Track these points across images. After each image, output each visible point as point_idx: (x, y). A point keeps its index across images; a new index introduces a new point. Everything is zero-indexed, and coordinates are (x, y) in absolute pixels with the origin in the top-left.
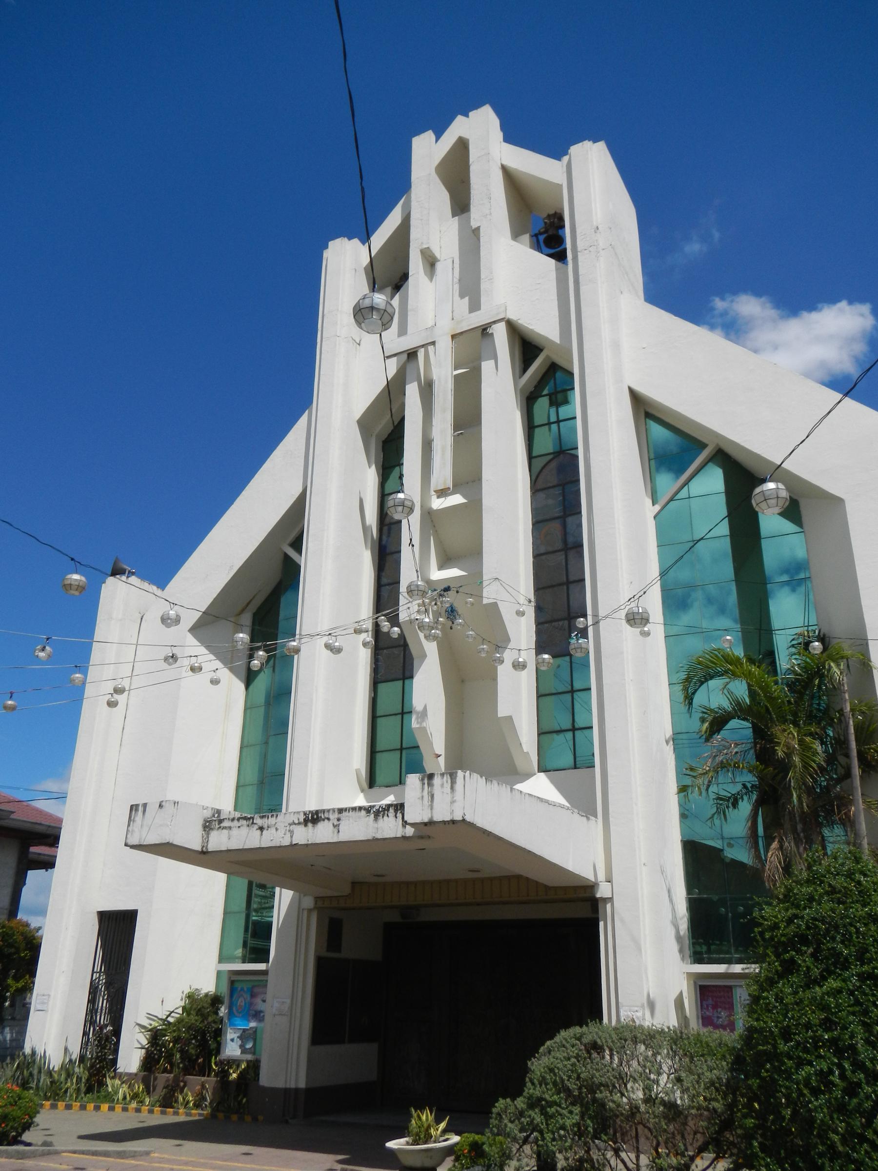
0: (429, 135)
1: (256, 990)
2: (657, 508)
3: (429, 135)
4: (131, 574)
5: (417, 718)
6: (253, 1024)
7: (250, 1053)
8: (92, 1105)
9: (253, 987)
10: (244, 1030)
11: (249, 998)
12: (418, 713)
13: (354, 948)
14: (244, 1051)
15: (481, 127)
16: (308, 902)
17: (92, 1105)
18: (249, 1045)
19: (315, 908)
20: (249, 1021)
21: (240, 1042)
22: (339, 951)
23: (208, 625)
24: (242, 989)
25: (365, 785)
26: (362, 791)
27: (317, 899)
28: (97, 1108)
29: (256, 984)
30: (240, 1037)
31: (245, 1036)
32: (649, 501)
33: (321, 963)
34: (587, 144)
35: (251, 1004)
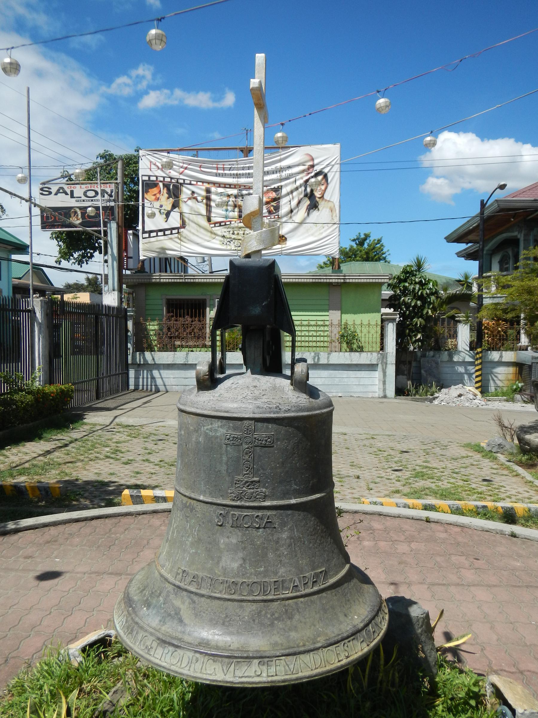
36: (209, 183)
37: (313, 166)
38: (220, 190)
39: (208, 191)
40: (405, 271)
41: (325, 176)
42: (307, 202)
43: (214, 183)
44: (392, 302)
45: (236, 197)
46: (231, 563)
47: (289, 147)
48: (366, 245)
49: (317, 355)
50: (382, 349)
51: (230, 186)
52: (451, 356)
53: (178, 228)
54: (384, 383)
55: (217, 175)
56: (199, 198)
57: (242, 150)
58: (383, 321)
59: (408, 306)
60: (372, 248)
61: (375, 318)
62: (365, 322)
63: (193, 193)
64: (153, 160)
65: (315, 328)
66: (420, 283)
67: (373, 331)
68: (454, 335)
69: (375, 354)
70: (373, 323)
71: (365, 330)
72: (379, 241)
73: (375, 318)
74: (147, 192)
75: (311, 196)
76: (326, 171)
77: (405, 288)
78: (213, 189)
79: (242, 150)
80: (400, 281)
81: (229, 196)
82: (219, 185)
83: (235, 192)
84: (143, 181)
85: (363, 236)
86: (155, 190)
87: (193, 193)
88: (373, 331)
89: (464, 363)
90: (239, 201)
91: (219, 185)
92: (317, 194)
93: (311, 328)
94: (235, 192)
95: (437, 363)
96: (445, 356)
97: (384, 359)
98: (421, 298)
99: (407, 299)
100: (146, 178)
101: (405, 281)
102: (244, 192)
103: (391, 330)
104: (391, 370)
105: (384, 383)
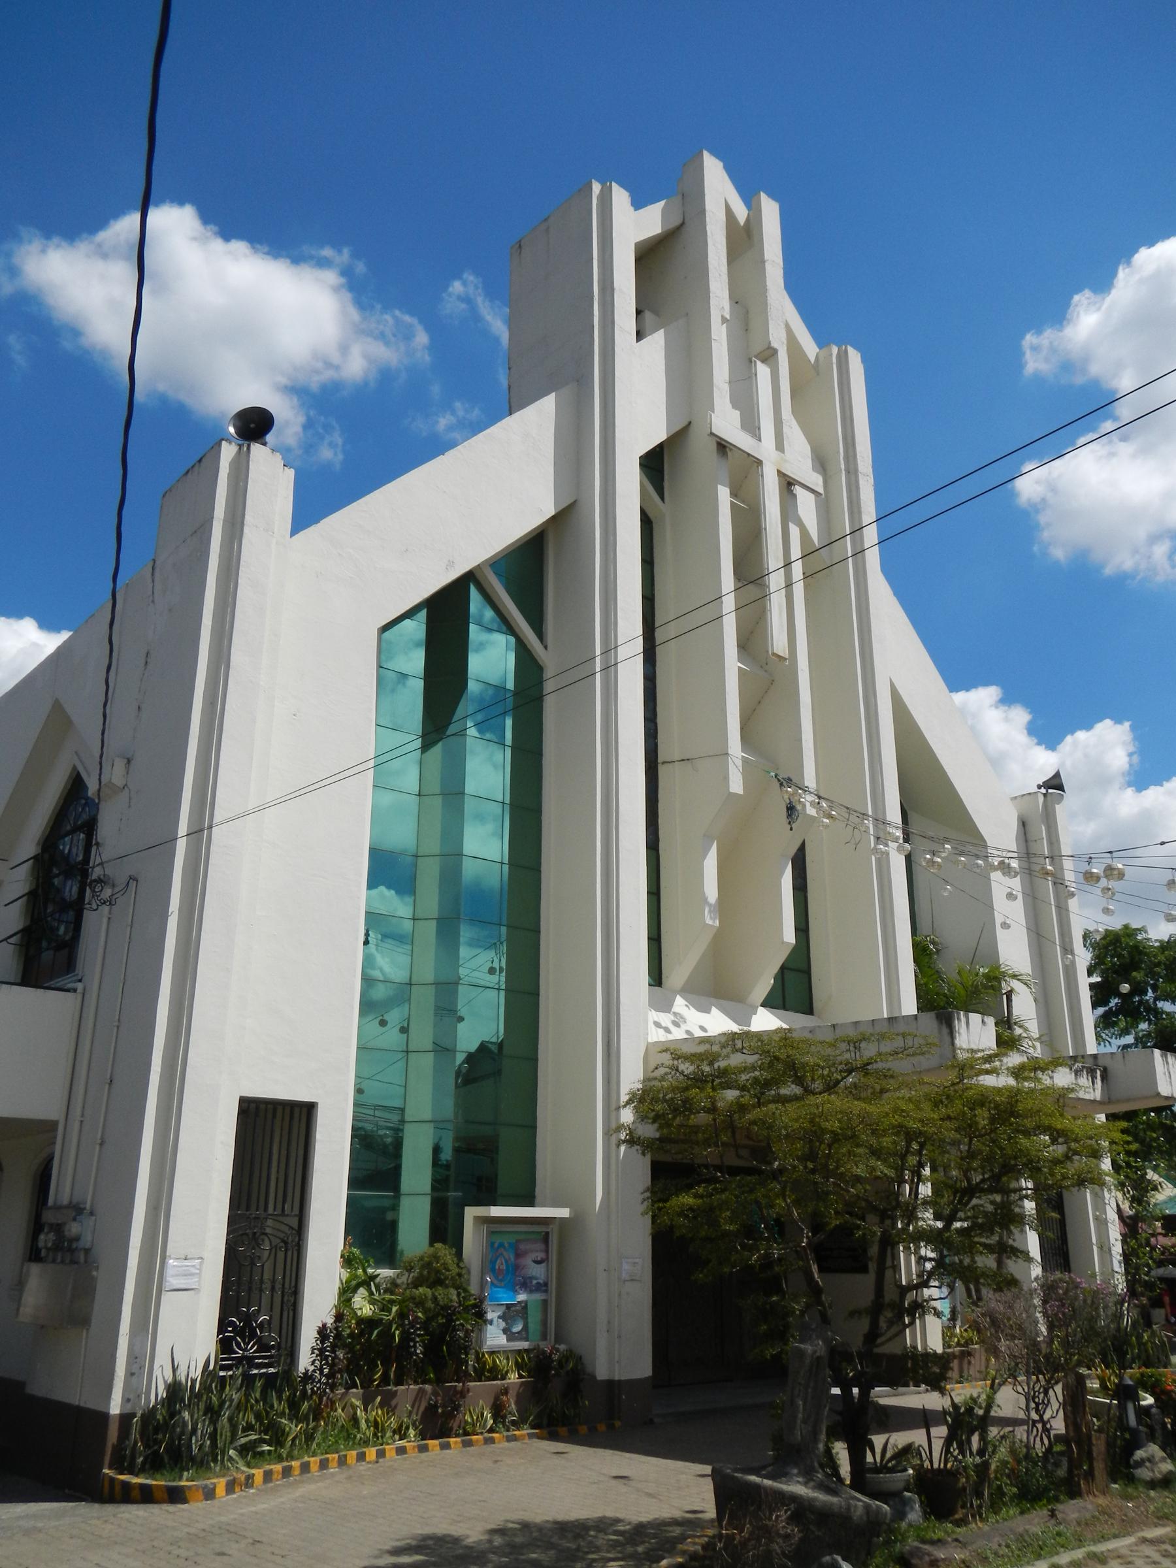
1: (522, 1247)
5: (710, 912)
6: (522, 1297)
7: (521, 1339)
8: (354, 1453)
9: (518, 1241)
10: (508, 1306)
11: (512, 1257)
12: (710, 905)
14: (511, 1337)
17: (354, 1453)
18: (517, 1328)
20: (516, 1292)
21: (503, 1324)
24: (501, 1245)
28: (342, 1462)
29: (522, 1237)
30: (503, 1317)
31: (509, 1313)
35: (517, 1268)
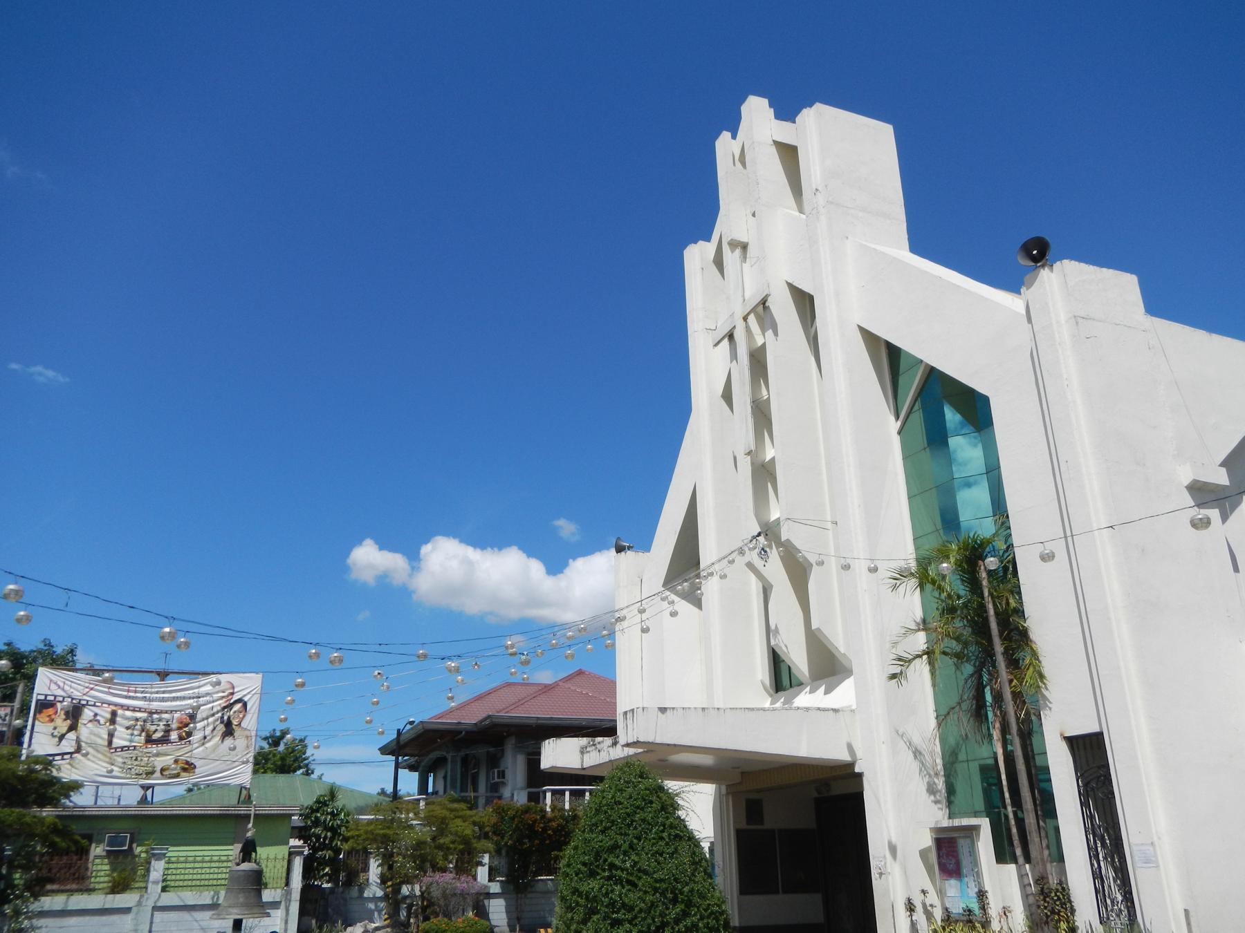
0: (726, 135)
2: (899, 423)
3: (726, 135)
4: (629, 548)
13: (773, 820)
15: (757, 112)
16: (724, 788)
19: (728, 794)
22: (762, 823)
23: (671, 580)
25: (772, 692)
26: (771, 696)
27: (728, 786)
32: (892, 418)
33: (740, 834)
34: (805, 111)
36: (116, 705)
37: (232, 694)
38: (128, 713)
39: (114, 714)
40: (318, 801)
41: (245, 705)
42: (221, 728)
43: (122, 706)
44: (301, 833)
45: (145, 721)
46: (241, 900)
47: (208, 674)
48: (281, 748)
49: (217, 893)
50: (287, 884)
51: (140, 710)
52: (361, 891)
53: (71, 753)
54: (286, 922)
55: (126, 697)
56: (102, 721)
57: (158, 673)
58: (290, 854)
59: (318, 837)
60: (291, 750)
61: (282, 851)
62: (272, 856)
63: (96, 715)
64: (54, 678)
65: (217, 864)
66: (332, 813)
67: (279, 866)
68: (366, 869)
69: (279, 891)
70: (280, 856)
71: (270, 865)
72: (301, 741)
73: (282, 851)
74: (40, 712)
75: (228, 724)
76: (246, 699)
77: (316, 818)
78: (120, 712)
79: (158, 673)
80: (313, 811)
81: (137, 720)
82: (128, 708)
83: (144, 715)
84: (38, 701)
85: (278, 734)
86: (51, 711)
87: (96, 715)
88: (279, 866)
89: (375, 899)
90: (148, 726)
91: (128, 708)
92: (235, 722)
93: (213, 865)
94: (144, 715)
95: (345, 900)
96: (354, 892)
97: (288, 894)
98: (334, 830)
99: (318, 830)
100: (42, 697)
101: (317, 811)
102: (155, 716)
103: (298, 863)
104: (295, 908)
105: (286, 922)
